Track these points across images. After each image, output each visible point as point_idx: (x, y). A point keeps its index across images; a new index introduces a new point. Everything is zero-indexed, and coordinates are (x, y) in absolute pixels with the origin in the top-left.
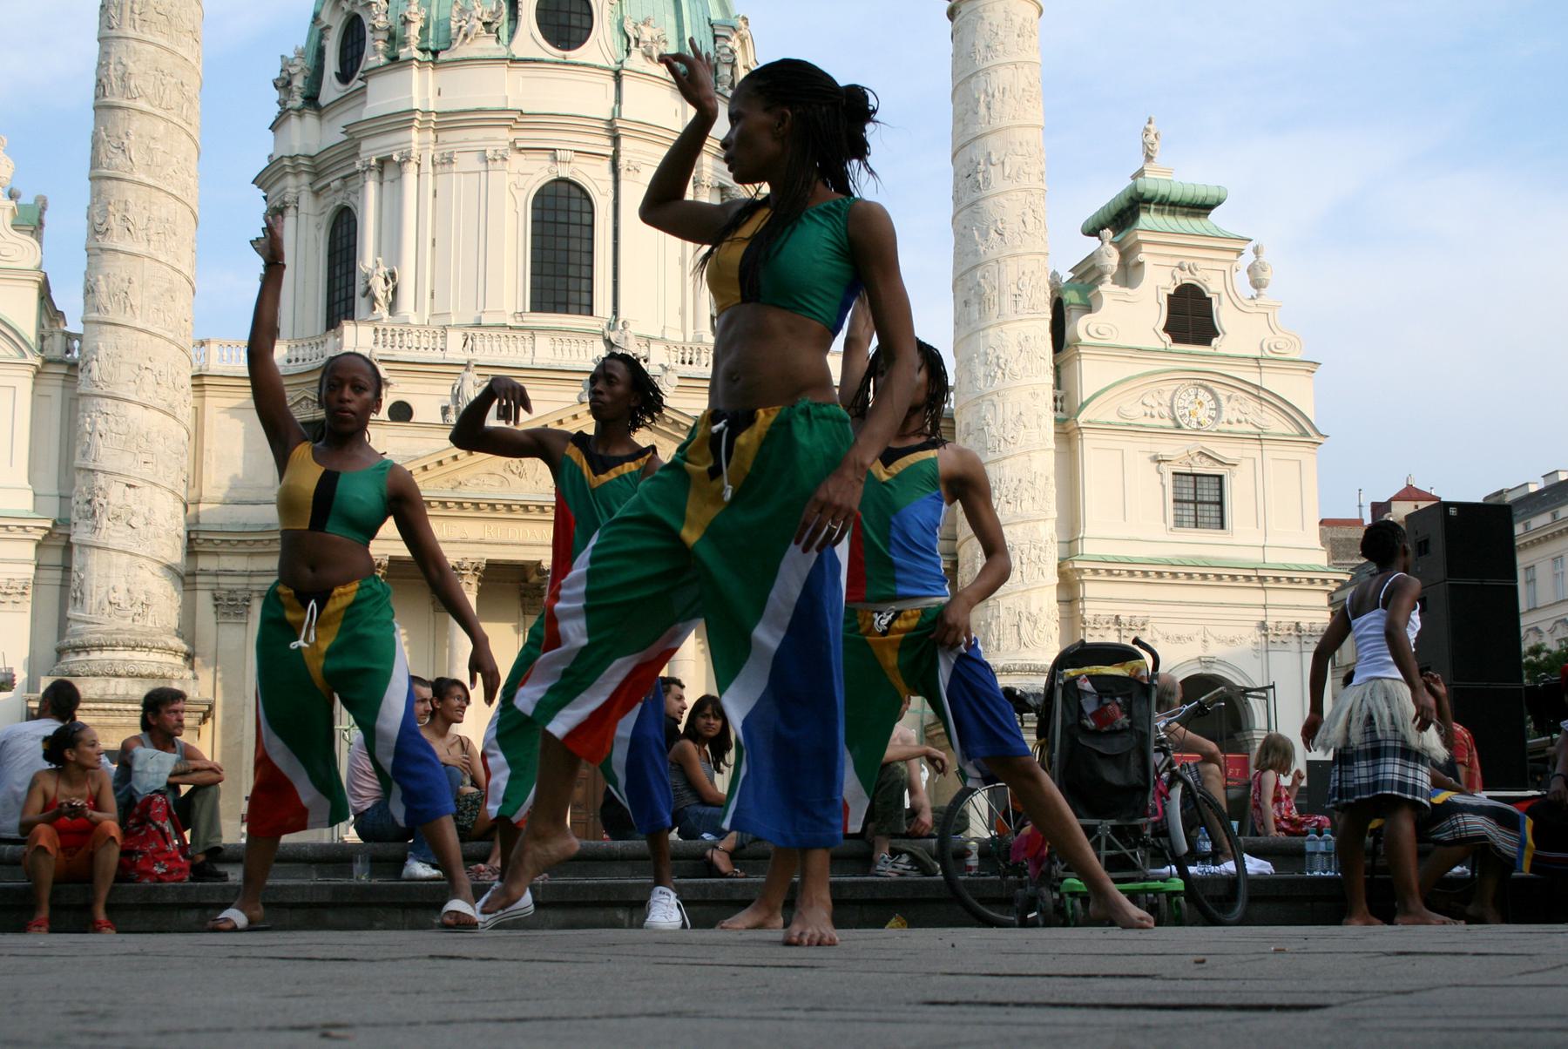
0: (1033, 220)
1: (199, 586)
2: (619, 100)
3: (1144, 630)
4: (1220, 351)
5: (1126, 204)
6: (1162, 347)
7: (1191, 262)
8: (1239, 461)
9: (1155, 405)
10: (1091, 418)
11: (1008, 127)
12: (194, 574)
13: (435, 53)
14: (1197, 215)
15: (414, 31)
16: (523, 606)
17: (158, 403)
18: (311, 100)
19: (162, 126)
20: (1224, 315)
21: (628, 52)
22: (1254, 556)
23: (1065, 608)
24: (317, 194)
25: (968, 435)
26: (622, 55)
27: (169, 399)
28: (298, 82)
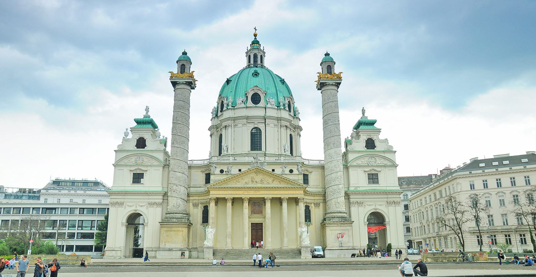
2: (266, 113)
4: (377, 150)
5: (358, 124)
7: (370, 134)
10: (351, 164)
13: (234, 107)
14: (371, 125)
15: (230, 104)
18: (217, 115)
19: (182, 125)
20: (377, 143)
21: (267, 104)
22: (385, 188)
23: (347, 200)
24: (217, 132)
25: (326, 169)
28: (214, 113)
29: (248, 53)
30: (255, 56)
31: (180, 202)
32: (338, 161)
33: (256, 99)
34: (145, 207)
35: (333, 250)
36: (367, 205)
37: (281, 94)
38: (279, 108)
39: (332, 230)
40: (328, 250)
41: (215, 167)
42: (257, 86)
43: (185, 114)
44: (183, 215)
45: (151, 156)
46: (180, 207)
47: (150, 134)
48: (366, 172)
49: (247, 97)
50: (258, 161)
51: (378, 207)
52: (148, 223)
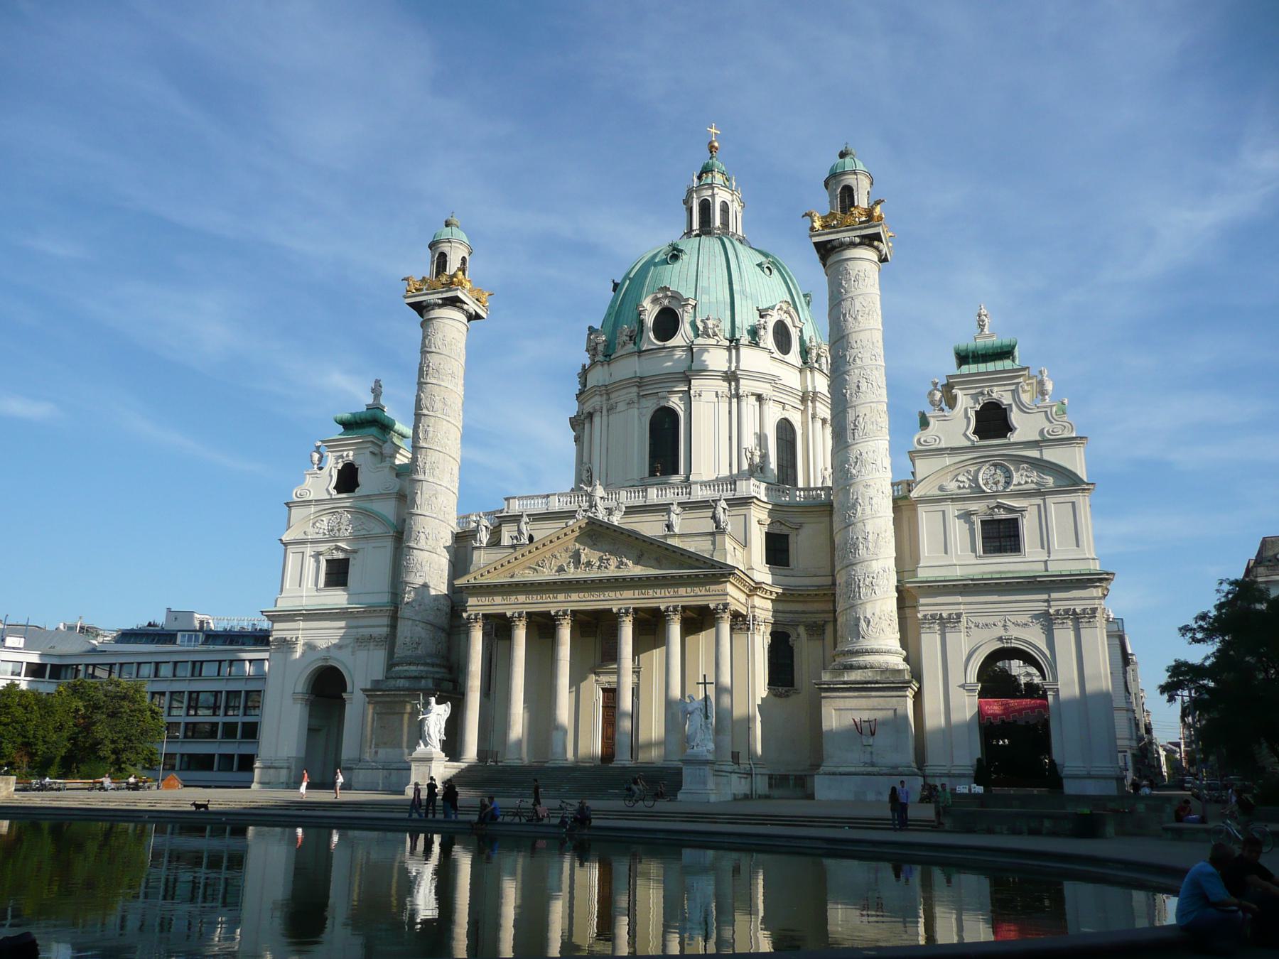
0: (866, 384)
1: (462, 632)
2: (692, 362)
3: (960, 621)
6: (968, 444)
8: (1027, 507)
9: (966, 480)
10: (922, 493)
11: (848, 335)
12: (459, 627)
13: (610, 356)
15: (600, 348)
16: (581, 633)
17: (425, 548)
19: (433, 420)
20: (1015, 417)
22: (1038, 569)
26: (692, 335)
27: (433, 546)
29: (688, 202)
30: (706, 207)
31: (421, 632)
32: (866, 486)
33: (668, 323)
34: (350, 649)
35: (841, 774)
36: (978, 626)
37: (749, 301)
38: (733, 344)
39: (842, 709)
40: (825, 774)
41: (485, 526)
42: (667, 289)
43: (442, 388)
44: (431, 669)
45: (366, 511)
46: (421, 646)
47: (367, 452)
48: (974, 518)
49: (641, 323)
50: (598, 500)
51: (1014, 632)
52: (352, 693)
